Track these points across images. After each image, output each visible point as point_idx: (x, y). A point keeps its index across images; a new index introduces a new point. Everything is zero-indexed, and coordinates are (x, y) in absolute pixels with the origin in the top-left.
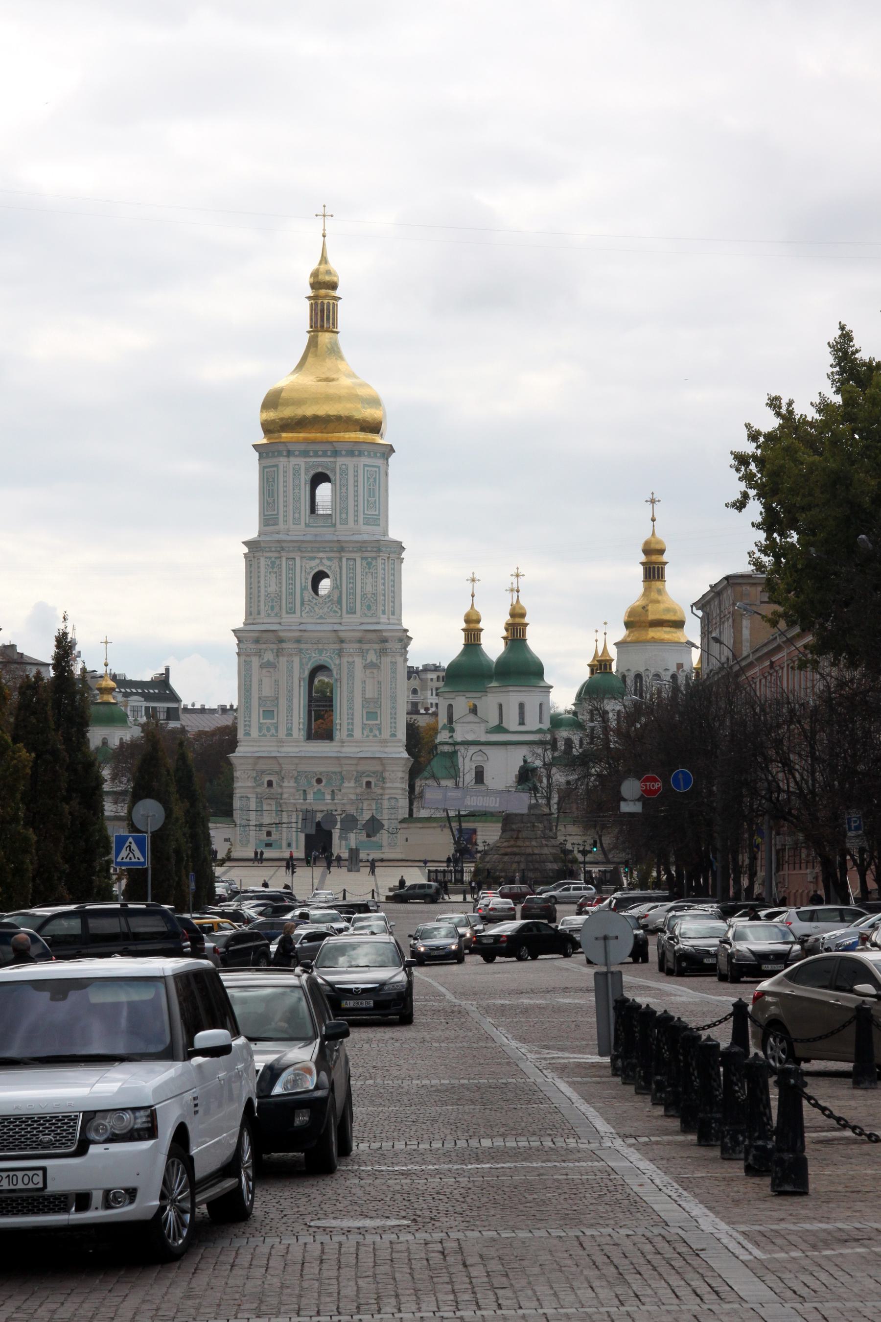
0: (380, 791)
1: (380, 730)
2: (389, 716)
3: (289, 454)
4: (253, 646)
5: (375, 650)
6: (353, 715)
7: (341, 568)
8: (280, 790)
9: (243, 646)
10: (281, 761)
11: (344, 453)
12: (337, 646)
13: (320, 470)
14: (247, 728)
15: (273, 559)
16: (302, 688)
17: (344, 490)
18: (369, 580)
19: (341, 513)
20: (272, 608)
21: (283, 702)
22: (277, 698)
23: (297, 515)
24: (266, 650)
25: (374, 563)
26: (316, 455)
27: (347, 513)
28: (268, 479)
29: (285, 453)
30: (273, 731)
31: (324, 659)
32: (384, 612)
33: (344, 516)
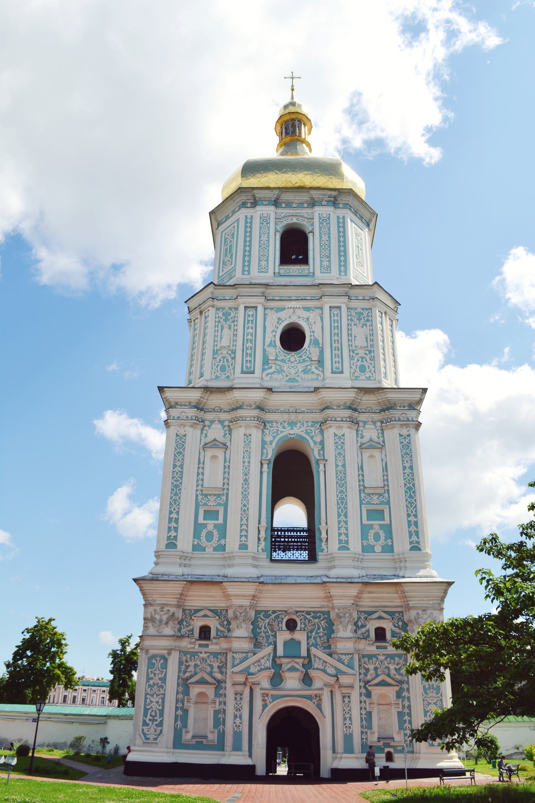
3: (255, 204)
4: (191, 412)
9: (174, 412)
11: (324, 203)
13: (295, 220)
14: (173, 534)
16: (265, 475)
17: (325, 238)
19: (321, 261)
20: (223, 368)
23: (263, 263)
26: (289, 205)
27: (329, 261)
28: (226, 239)
29: (249, 205)
31: (300, 431)
32: (386, 377)
33: (326, 263)
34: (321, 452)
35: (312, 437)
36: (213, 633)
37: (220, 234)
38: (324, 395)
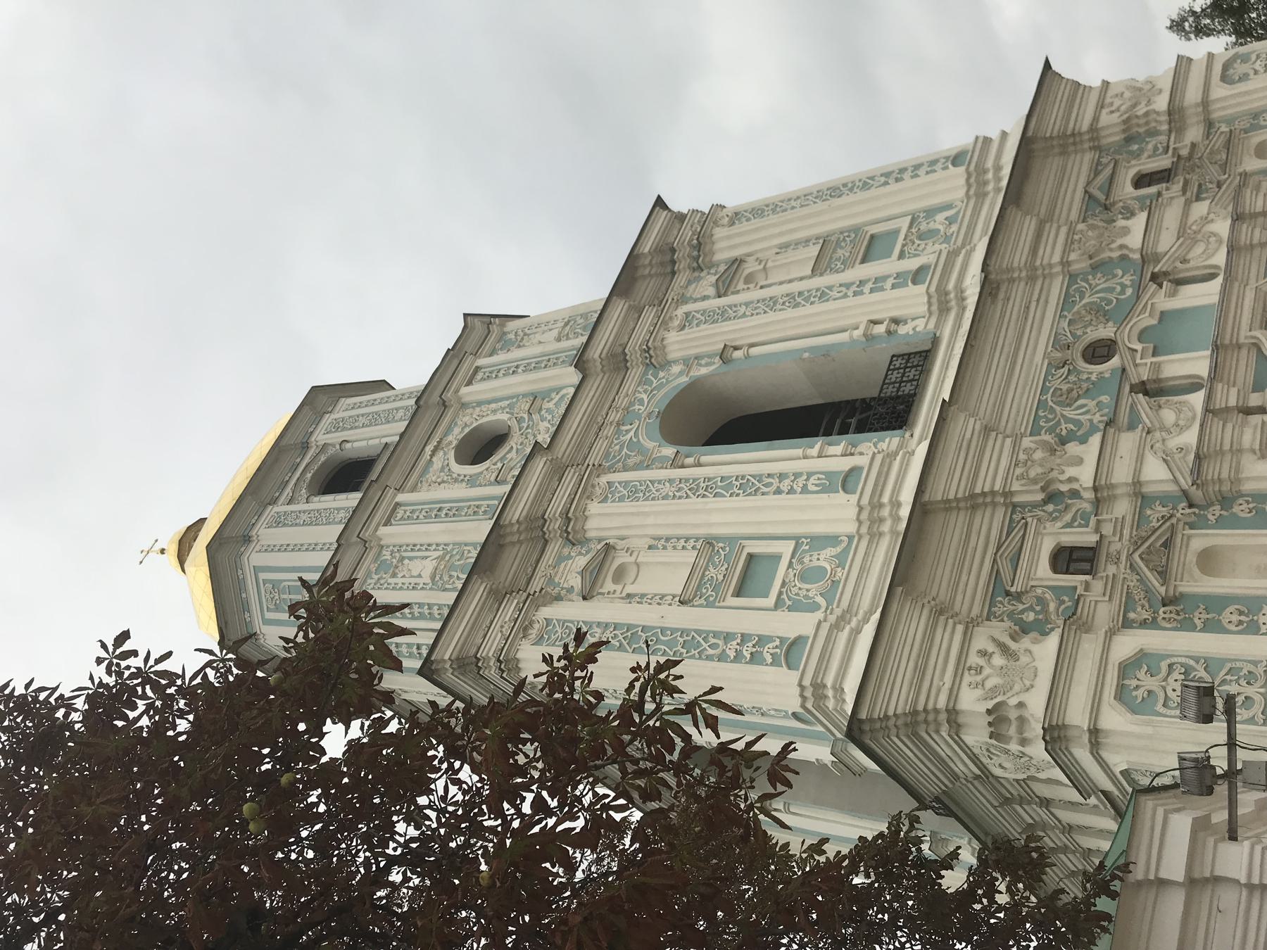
0: (1194, 133)
1: (930, 213)
2: (888, 188)
4: (509, 610)
5: (689, 282)
6: (848, 286)
7: (479, 404)
8: (1122, 508)
10: (947, 486)
12: (635, 373)
15: (373, 568)
18: (538, 337)
21: (725, 516)
22: (710, 542)
24: (551, 579)
25: (512, 336)
30: (824, 559)
34: (703, 362)
35: (668, 382)
36: (1084, 537)
37: (266, 629)
38: (596, 356)
